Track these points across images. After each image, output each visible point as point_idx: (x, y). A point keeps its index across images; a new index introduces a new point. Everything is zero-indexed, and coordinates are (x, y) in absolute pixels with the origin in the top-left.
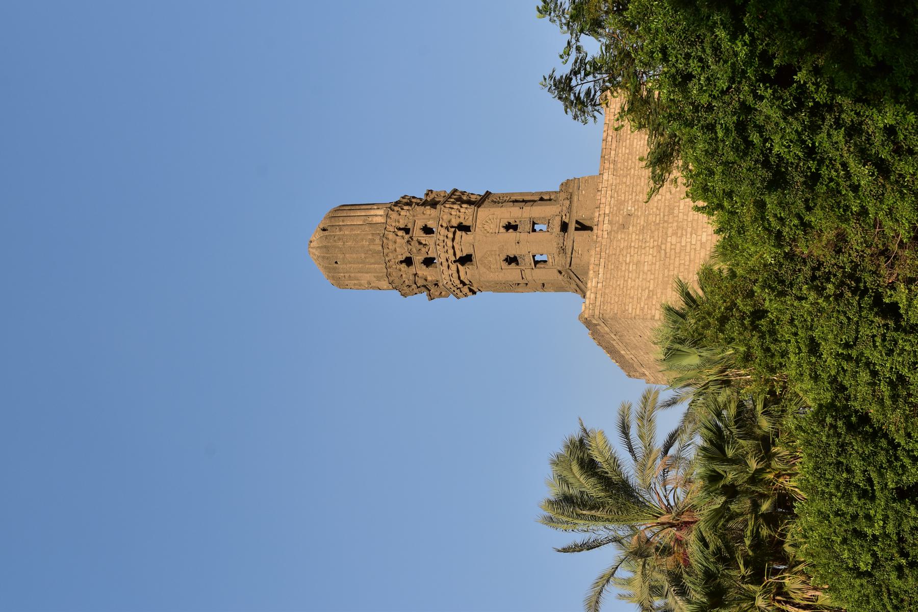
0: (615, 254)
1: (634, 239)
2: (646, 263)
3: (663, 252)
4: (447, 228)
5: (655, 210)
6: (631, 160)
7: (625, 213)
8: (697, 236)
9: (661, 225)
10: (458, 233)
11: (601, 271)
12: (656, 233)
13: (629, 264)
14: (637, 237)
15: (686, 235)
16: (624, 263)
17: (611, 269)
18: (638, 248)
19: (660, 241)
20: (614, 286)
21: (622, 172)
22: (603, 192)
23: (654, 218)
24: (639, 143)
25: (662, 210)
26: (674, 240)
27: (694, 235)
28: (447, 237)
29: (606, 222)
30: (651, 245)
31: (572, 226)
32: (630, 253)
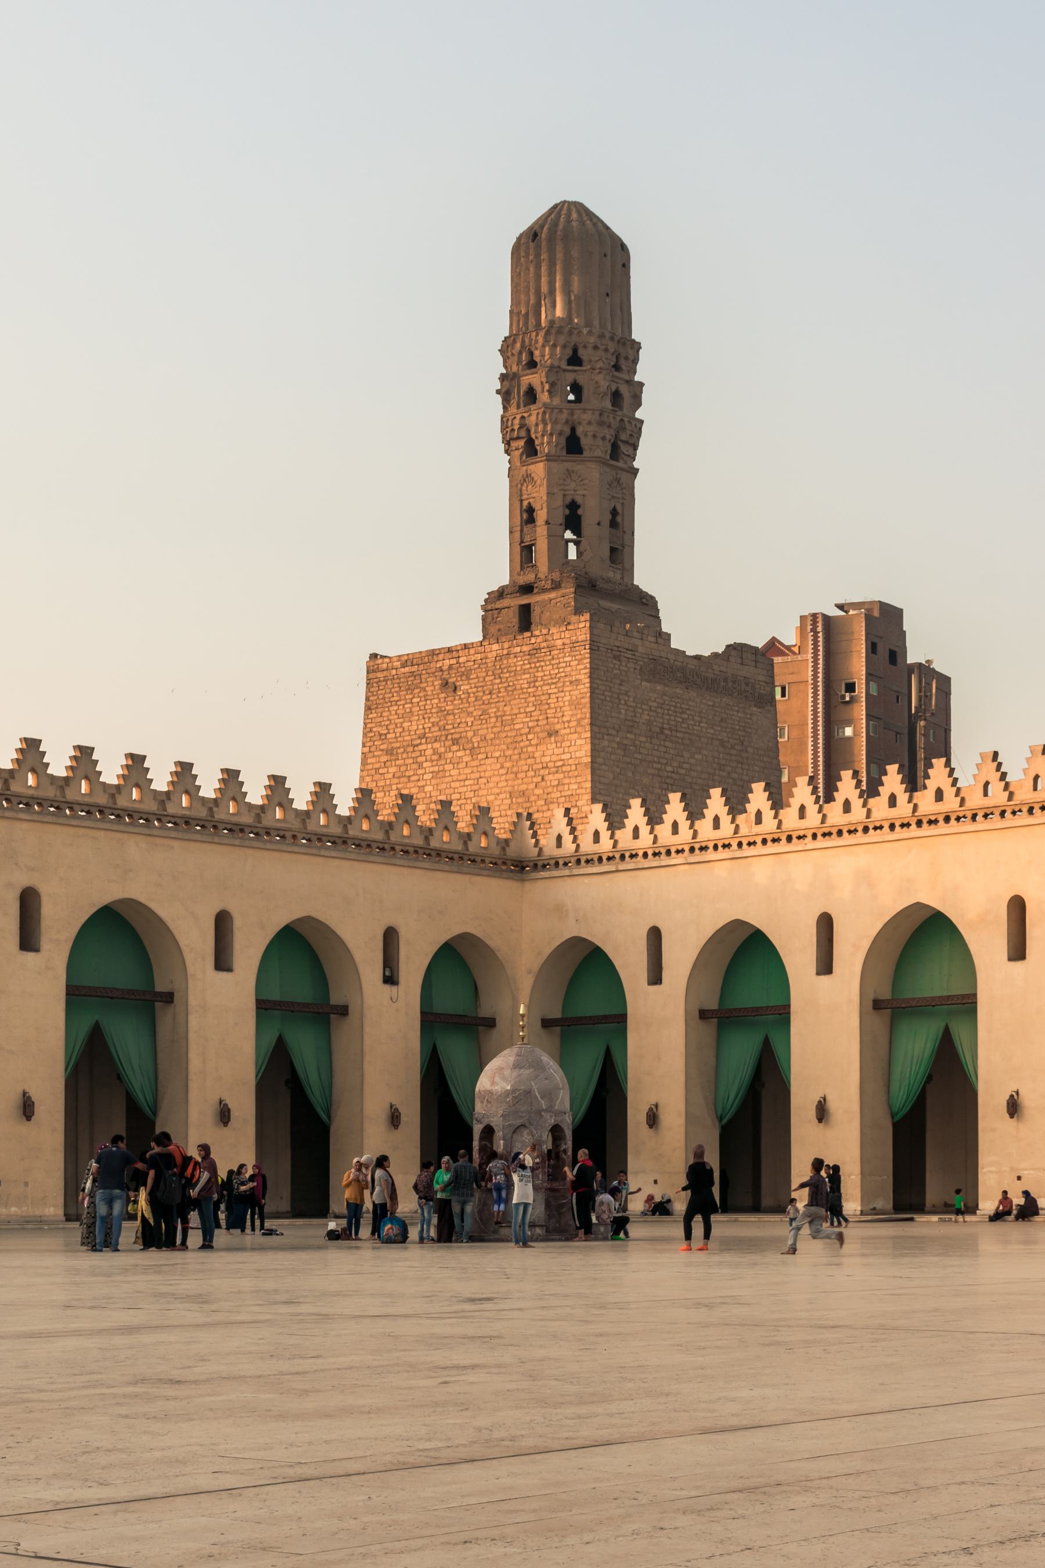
0: (421, 682)
1: (433, 702)
2: (410, 724)
3: (418, 742)
4: (521, 426)
5: (458, 721)
6: (510, 677)
7: (458, 684)
8: (430, 780)
9: (443, 733)
10: (521, 443)
11: (407, 669)
12: (437, 728)
13: (411, 703)
14: (435, 706)
15: (433, 766)
16: (411, 696)
17: (407, 682)
18: (425, 709)
19: (430, 735)
20: (393, 690)
21: (498, 667)
22: (480, 648)
23: (450, 722)
24: (525, 682)
25: (457, 730)
26: (429, 752)
27: (431, 775)
28: (513, 430)
29: (453, 661)
30: (426, 726)
31: (525, 600)
32: (421, 701)
